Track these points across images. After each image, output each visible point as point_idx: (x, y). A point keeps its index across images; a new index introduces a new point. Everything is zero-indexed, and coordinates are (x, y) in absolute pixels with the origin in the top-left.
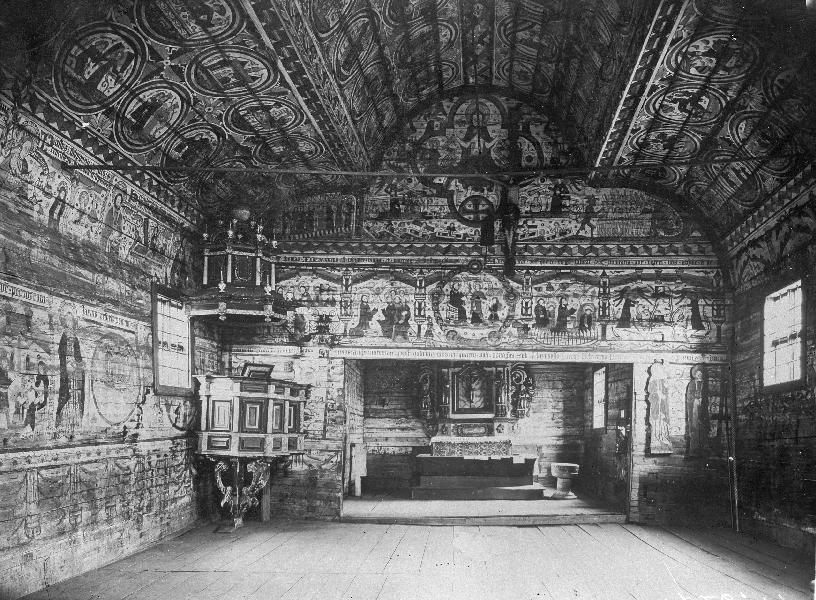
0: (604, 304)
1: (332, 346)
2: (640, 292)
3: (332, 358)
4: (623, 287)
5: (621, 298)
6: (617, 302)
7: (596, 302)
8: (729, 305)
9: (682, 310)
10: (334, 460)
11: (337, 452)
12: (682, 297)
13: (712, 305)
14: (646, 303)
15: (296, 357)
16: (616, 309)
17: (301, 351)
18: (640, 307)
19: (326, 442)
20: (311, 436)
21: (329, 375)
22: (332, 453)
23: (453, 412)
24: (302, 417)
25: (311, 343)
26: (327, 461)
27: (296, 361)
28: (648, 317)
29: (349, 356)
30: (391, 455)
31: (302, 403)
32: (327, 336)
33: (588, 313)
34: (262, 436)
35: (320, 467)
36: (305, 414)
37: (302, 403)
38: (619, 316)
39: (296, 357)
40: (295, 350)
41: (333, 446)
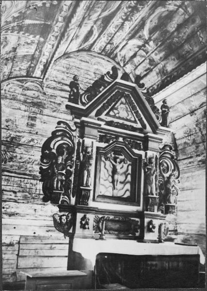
23: (94, 200)
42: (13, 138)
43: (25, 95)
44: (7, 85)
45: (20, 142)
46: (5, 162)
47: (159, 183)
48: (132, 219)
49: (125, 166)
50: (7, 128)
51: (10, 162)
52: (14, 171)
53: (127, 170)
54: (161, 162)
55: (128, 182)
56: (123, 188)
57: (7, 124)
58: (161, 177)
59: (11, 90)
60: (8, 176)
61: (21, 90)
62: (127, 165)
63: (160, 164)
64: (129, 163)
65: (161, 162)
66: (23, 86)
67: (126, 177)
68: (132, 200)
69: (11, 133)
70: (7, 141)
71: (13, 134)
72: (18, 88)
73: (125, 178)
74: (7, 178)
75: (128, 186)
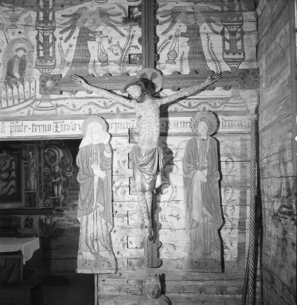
0: (46, 38)
2: (103, 14)
4: (74, 9)
5: (73, 27)
6: (68, 33)
7: (32, 35)
8: (249, 33)
9: (172, 44)
12: (174, 22)
13: (222, 33)
14: (113, 33)
16: (65, 46)
18: (106, 45)
28: (118, 58)
33: (21, 54)
38: (70, 57)
47: (44, 175)
48: (13, 216)
49: (8, 162)
53: (11, 166)
54: (46, 151)
55: (13, 178)
56: (7, 185)
58: (47, 168)
62: (10, 161)
63: (44, 154)
64: (11, 158)
65: (46, 151)
67: (10, 174)
68: (16, 197)
73: (8, 175)
75: (13, 183)
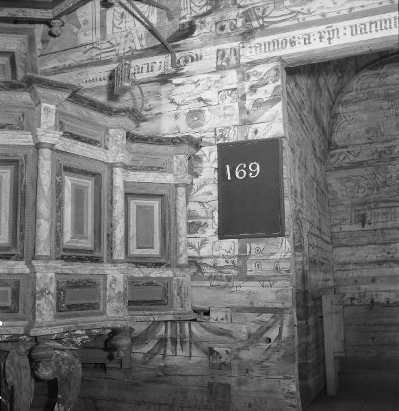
1: (247, 35)
3: (253, 64)
10: (273, 334)
11: (277, 312)
15: (164, 79)
17: (175, 63)
19: (248, 286)
20: (208, 271)
21: (242, 108)
22: (267, 317)
24: (183, 225)
25: (194, 40)
26: (253, 338)
27: (165, 89)
29: (287, 51)
30: (383, 306)
31: (181, 190)
32: (233, 14)
34: (20, 267)
35: (236, 358)
36: (191, 215)
37: (181, 190)
39: (164, 79)
40: (161, 63)
41: (267, 295)
42: (380, 153)
43: (384, 85)
44: (357, 82)
45: (393, 156)
46: (378, 189)
50: (370, 141)
51: (383, 187)
52: (392, 199)
57: (369, 136)
59: (364, 86)
60: (386, 207)
61: (377, 80)
66: (378, 74)
69: (377, 146)
70: (374, 159)
71: (380, 147)
72: (372, 79)
74: (385, 210)
